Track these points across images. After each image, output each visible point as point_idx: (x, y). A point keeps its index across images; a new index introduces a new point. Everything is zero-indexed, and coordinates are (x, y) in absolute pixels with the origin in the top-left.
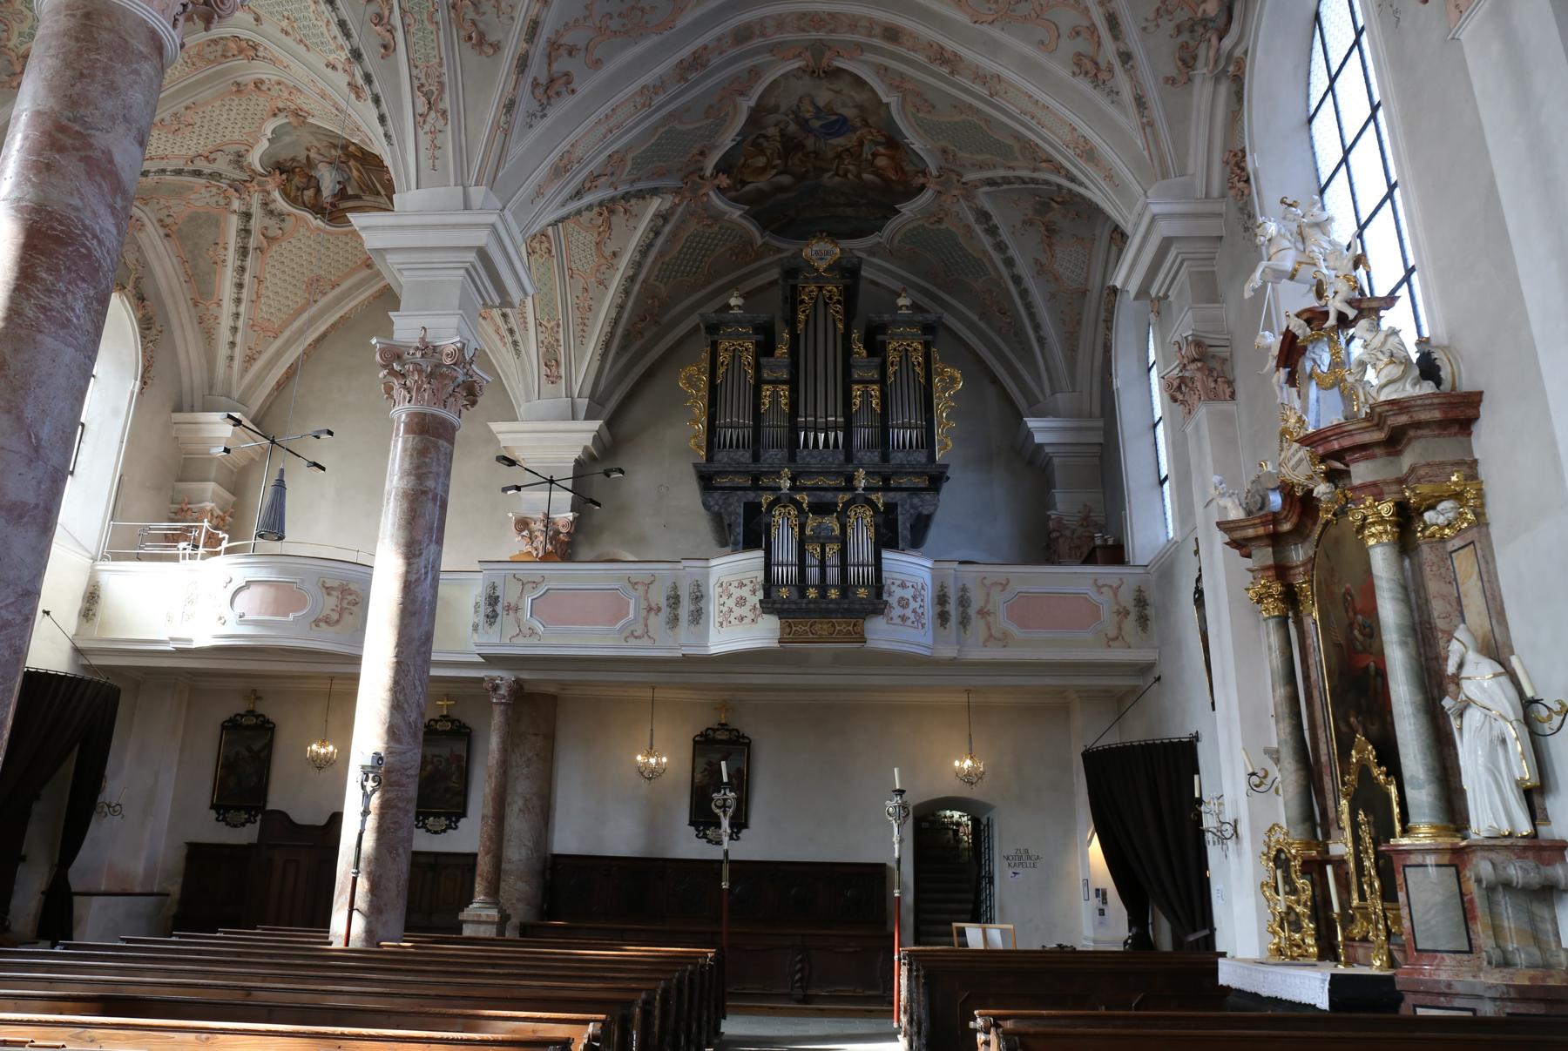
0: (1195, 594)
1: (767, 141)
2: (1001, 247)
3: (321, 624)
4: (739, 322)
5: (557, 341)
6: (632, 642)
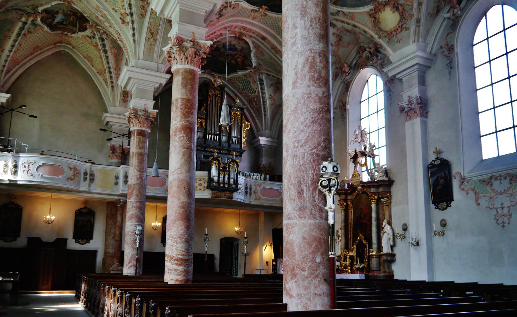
2: (262, 89)
3: (69, 180)
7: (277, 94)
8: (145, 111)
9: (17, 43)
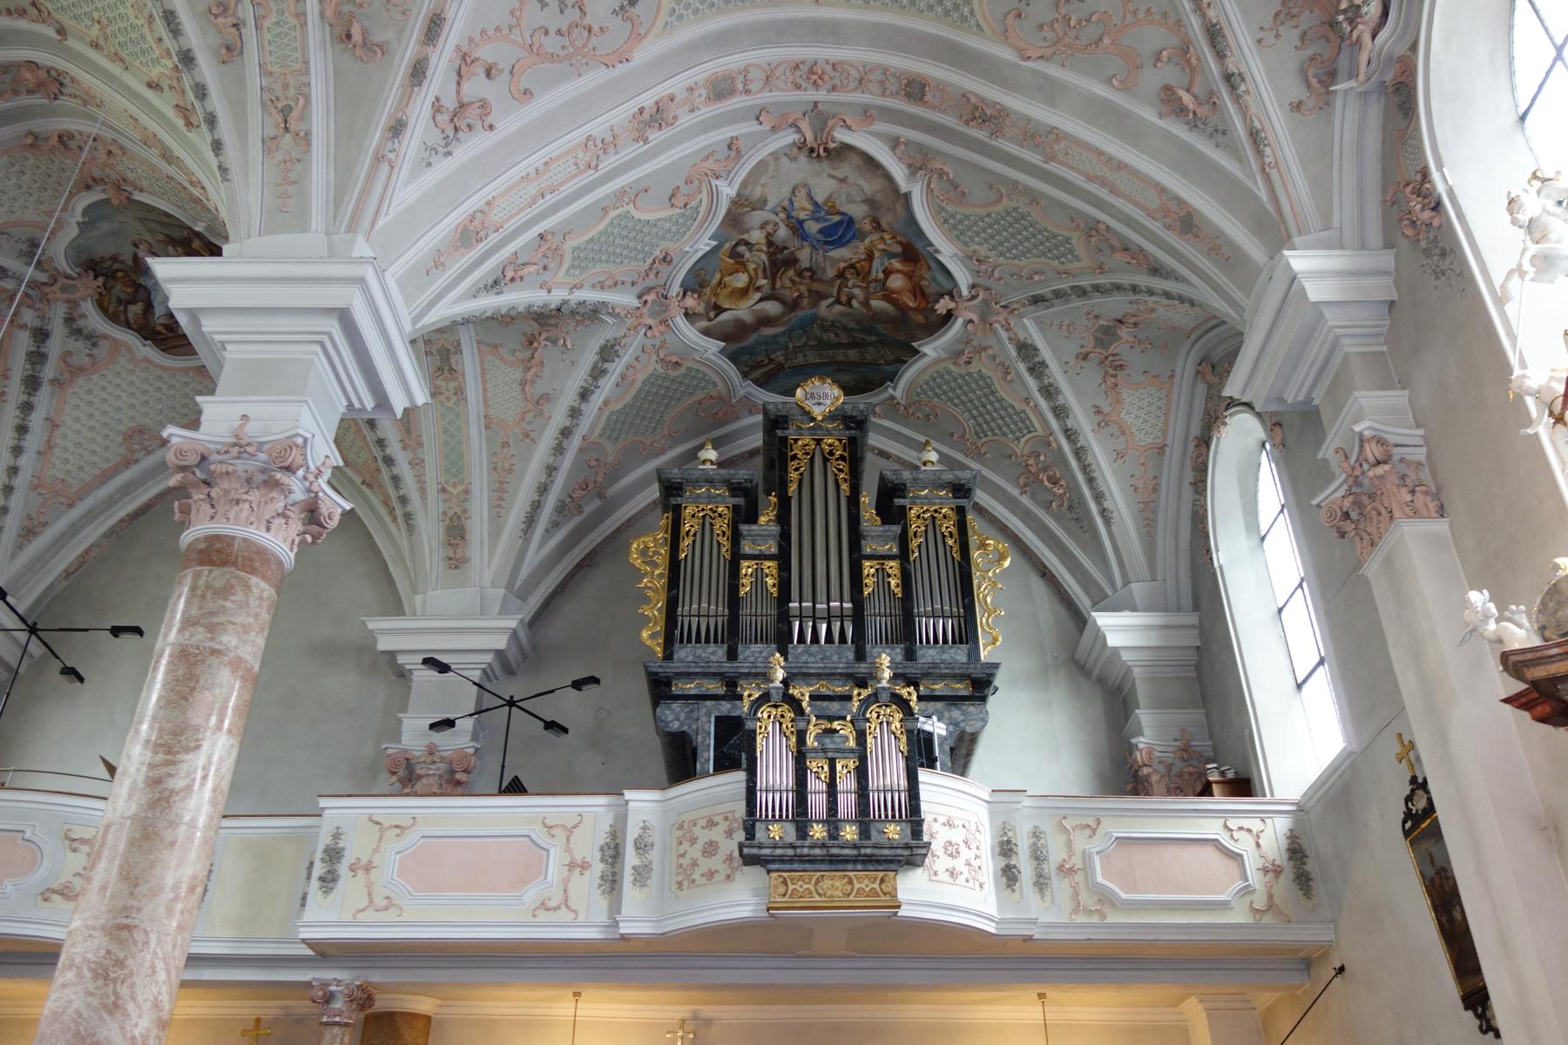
0: (1404, 822)
1: (750, 251)
2: (1049, 392)
3: (56, 897)
4: (710, 481)
5: (465, 511)
6: (544, 916)
7: (1126, 394)
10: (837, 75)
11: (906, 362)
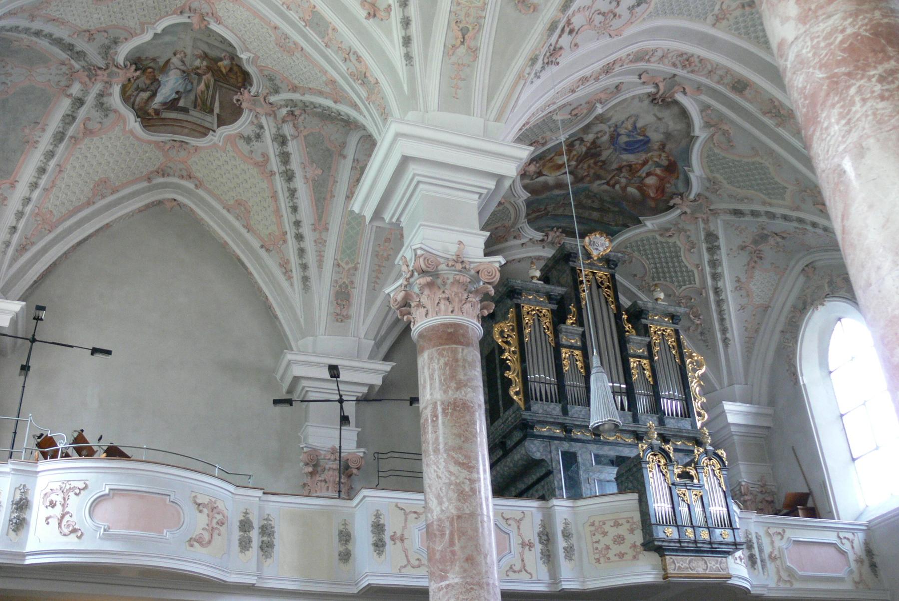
2: (714, 263)
4: (538, 291)
5: (352, 282)
6: (513, 576)
7: (757, 273)
8: (459, 259)
9: (53, 163)
10: (700, 65)
11: (629, 227)
